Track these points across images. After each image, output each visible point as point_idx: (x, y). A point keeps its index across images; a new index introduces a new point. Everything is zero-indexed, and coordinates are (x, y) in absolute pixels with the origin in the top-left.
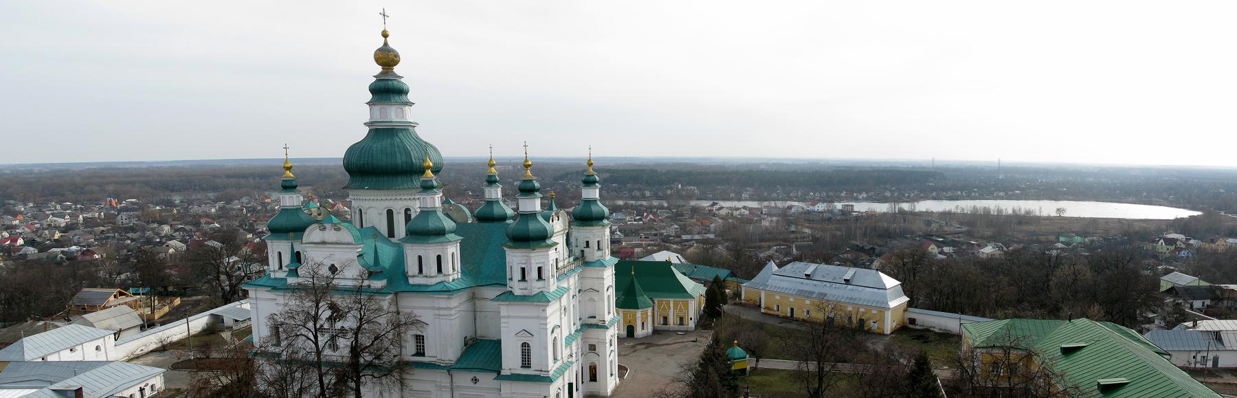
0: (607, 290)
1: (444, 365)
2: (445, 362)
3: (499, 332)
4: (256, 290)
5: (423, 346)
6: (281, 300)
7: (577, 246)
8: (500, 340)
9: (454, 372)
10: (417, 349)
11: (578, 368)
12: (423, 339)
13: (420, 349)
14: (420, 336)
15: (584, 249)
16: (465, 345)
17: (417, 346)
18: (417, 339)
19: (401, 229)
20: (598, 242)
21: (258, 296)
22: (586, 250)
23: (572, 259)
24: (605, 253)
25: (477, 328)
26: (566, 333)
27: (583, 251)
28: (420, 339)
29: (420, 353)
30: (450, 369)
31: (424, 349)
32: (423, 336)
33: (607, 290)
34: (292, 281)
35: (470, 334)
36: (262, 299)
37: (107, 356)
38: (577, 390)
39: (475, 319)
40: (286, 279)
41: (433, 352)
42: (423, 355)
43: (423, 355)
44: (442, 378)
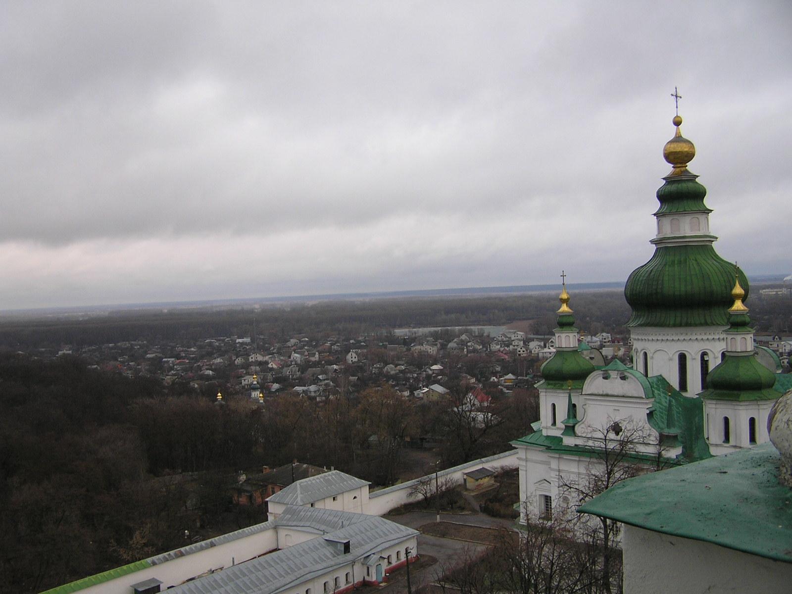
4: (526, 449)
6: (554, 464)
19: (695, 386)
21: (529, 457)
34: (569, 441)
36: (532, 461)
37: (362, 511)
40: (561, 440)
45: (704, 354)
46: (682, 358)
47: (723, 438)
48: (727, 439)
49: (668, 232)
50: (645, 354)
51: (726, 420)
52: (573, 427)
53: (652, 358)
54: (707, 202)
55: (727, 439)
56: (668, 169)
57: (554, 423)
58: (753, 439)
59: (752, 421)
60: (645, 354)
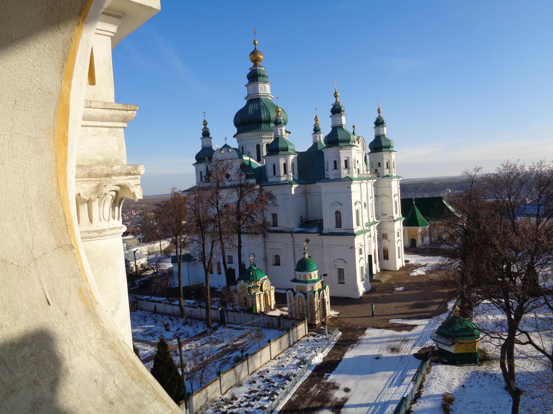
0: (395, 196)
1: (289, 231)
2: (289, 229)
3: (321, 214)
5: (277, 221)
7: (372, 168)
8: (322, 220)
9: (294, 235)
10: (273, 223)
11: (375, 248)
12: (277, 217)
13: (275, 223)
14: (275, 214)
15: (379, 169)
16: (302, 221)
17: (273, 221)
18: (273, 217)
20: (387, 163)
22: (379, 169)
23: (369, 172)
24: (392, 170)
25: (308, 212)
26: (366, 220)
27: (376, 170)
28: (275, 216)
29: (275, 224)
30: (291, 232)
31: (277, 223)
32: (276, 215)
33: (395, 196)
35: (304, 215)
38: (375, 262)
39: (307, 206)
41: (282, 224)
42: (277, 226)
43: (277, 226)
44: (286, 238)
45: (267, 145)
46: (258, 147)
47: (273, 174)
48: (275, 174)
49: (251, 93)
50: (242, 147)
51: (274, 165)
52: (209, 178)
53: (245, 148)
54: (269, 80)
55: (275, 174)
56: (252, 64)
57: (201, 180)
58: (285, 172)
59: (285, 165)
60: (242, 147)
